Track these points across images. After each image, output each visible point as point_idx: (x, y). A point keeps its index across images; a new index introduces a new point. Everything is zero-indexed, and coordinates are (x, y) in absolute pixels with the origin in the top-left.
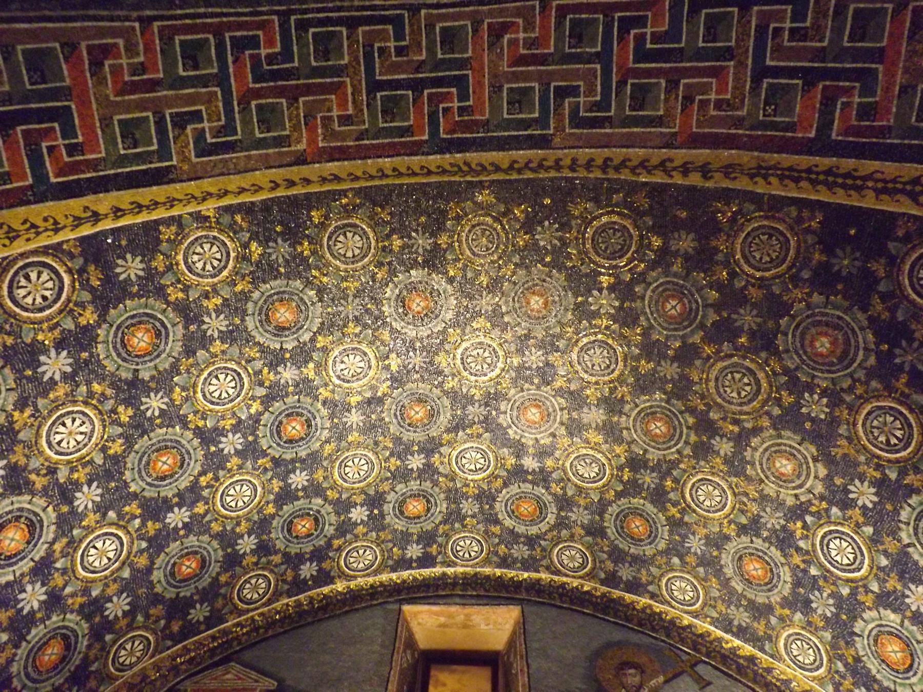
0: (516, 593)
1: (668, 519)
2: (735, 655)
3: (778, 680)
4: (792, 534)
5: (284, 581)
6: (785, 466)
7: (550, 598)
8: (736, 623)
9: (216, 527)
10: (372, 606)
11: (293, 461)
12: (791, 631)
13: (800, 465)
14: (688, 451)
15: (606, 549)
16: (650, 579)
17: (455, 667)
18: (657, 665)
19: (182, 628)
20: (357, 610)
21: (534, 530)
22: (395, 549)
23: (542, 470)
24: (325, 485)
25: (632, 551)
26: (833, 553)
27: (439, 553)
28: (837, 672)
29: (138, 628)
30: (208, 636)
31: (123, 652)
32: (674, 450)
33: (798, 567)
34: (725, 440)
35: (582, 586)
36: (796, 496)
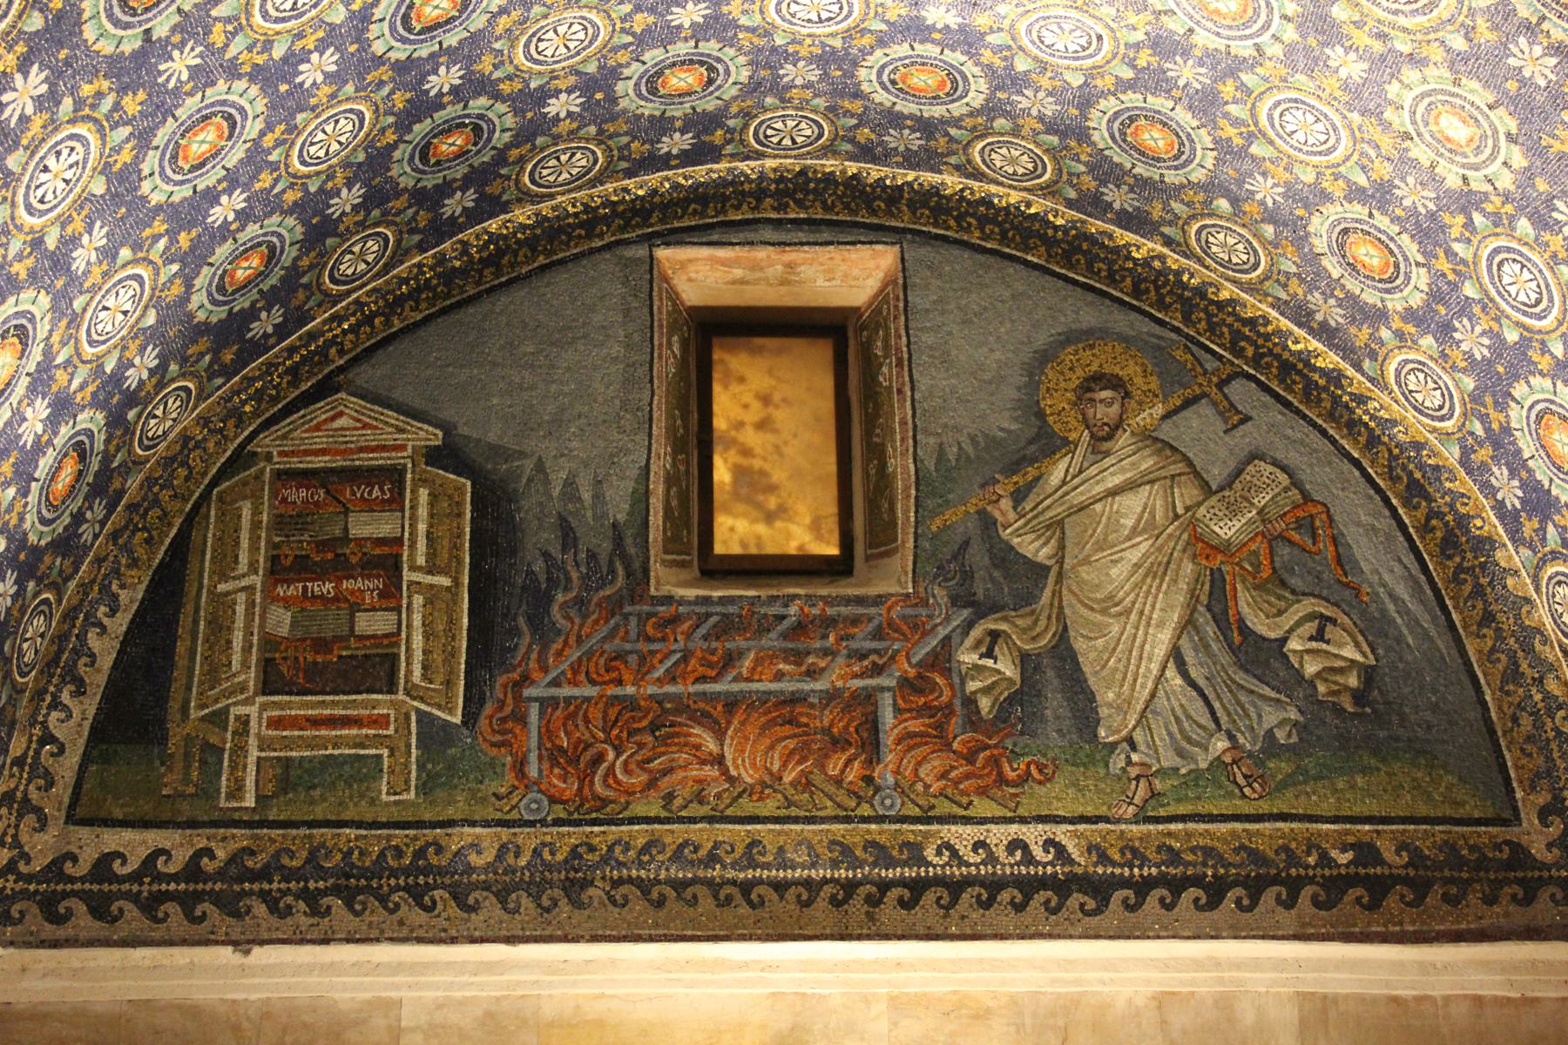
0: (892, 215)
1: (1215, 141)
2: (1307, 364)
3: (1373, 417)
4: (1443, 228)
5: (412, 232)
6: (1459, 132)
7: (960, 228)
8: (1319, 317)
9: (291, 197)
10: (592, 251)
11: (432, 56)
12: (1411, 357)
13: (1484, 137)
14: (1275, 50)
15: (1083, 158)
16: (1168, 217)
17: (759, 341)
18: (1154, 382)
19: (238, 354)
20: (561, 262)
21: (937, 111)
22: (635, 145)
23: (962, 29)
24: (497, 74)
25: (1137, 171)
26: (1506, 280)
27: (728, 142)
28: (1472, 434)
29: (173, 380)
30: (282, 350)
31: (153, 422)
32: (1250, 42)
33: (1444, 275)
34: (1352, 56)
35: (1029, 205)
36: (1465, 178)
